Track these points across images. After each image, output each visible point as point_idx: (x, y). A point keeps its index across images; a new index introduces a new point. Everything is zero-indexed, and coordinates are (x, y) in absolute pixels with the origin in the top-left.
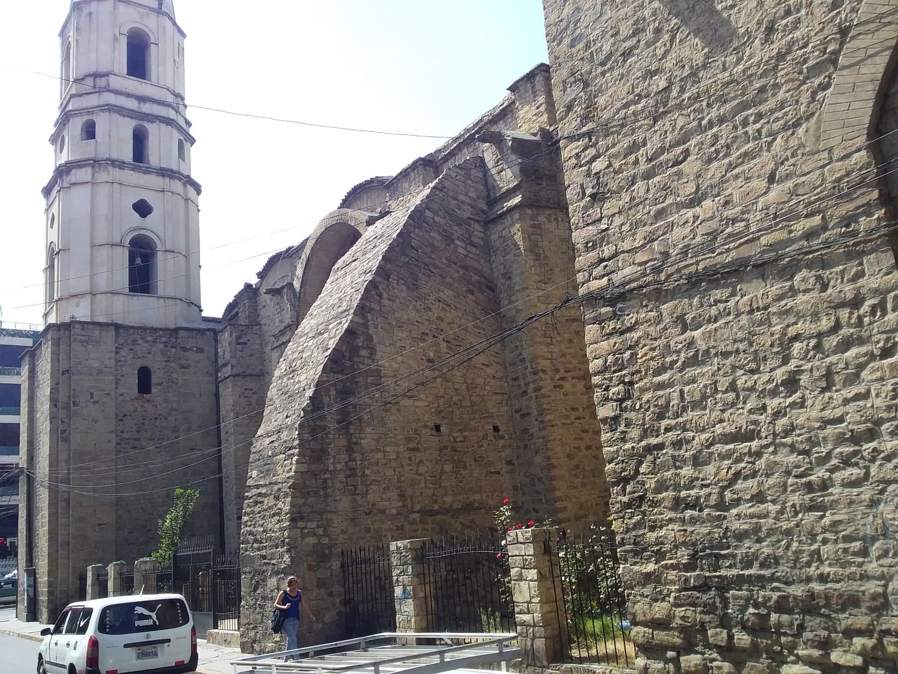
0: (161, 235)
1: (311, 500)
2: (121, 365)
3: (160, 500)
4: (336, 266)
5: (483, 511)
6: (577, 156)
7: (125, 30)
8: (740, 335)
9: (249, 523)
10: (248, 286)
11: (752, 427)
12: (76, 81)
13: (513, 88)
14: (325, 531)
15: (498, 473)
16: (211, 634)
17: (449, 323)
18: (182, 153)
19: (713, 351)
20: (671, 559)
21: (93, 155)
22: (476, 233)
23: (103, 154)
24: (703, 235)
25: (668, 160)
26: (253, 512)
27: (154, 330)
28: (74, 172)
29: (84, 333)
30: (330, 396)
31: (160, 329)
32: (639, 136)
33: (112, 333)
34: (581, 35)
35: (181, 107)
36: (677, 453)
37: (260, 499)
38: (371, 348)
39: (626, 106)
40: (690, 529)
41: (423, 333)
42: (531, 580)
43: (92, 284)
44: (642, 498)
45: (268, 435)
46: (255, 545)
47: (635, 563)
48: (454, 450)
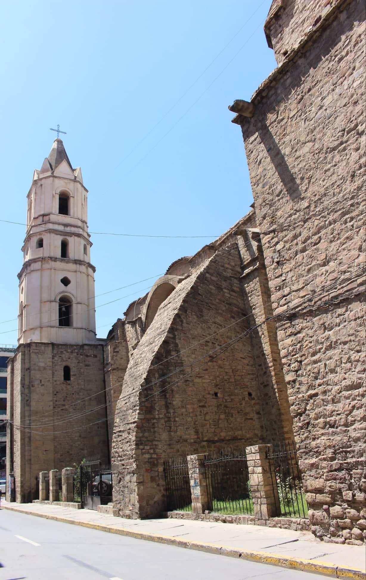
1: (146, 434)
2: (55, 365)
4: (160, 307)
5: (243, 441)
6: (269, 242)
8: (352, 332)
10: (119, 320)
11: (359, 381)
12: (34, 218)
14: (154, 451)
15: (252, 419)
16: (100, 508)
17: (221, 335)
19: (339, 341)
20: (323, 455)
21: (41, 256)
22: (235, 284)
23: (46, 255)
24: (331, 280)
25: (312, 243)
26: (117, 441)
27: (72, 346)
28: (32, 265)
29: (37, 348)
31: (75, 345)
32: (298, 230)
33: (50, 348)
34: (267, 182)
35: (85, 227)
36: (324, 398)
37: (120, 434)
38: (177, 351)
39: (290, 216)
40: (332, 438)
41: (207, 341)
42: (259, 473)
43: (41, 323)
44: (308, 423)
46: (119, 459)
47: (306, 459)
48: (226, 406)
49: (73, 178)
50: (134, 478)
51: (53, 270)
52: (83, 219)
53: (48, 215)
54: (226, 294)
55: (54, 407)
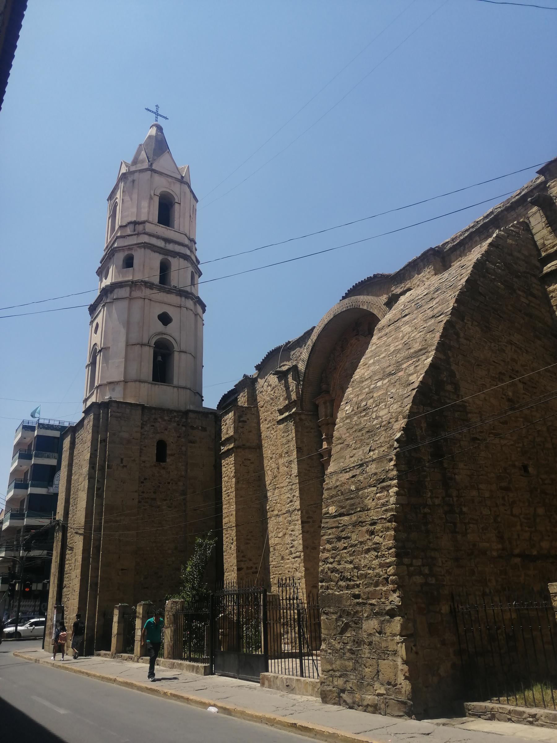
0: (178, 339)
3: (170, 552)
7: (158, 192)
9: (332, 560)
12: (121, 227)
13: (540, 172)
17: (522, 366)
18: (193, 283)
22: (534, 285)
26: (335, 549)
28: (116, 291)
30: (421, 429)
31: (175, 411)
33: (139, 412)
35: (194, 250)
41: (500, 373)
45: (345, 470)
49: (179, 177)
50: (397, 624)
51: (146, 301)
52: (191, 237)
53: (143, 223)
54: (523, 300)
55: (139, 502)
